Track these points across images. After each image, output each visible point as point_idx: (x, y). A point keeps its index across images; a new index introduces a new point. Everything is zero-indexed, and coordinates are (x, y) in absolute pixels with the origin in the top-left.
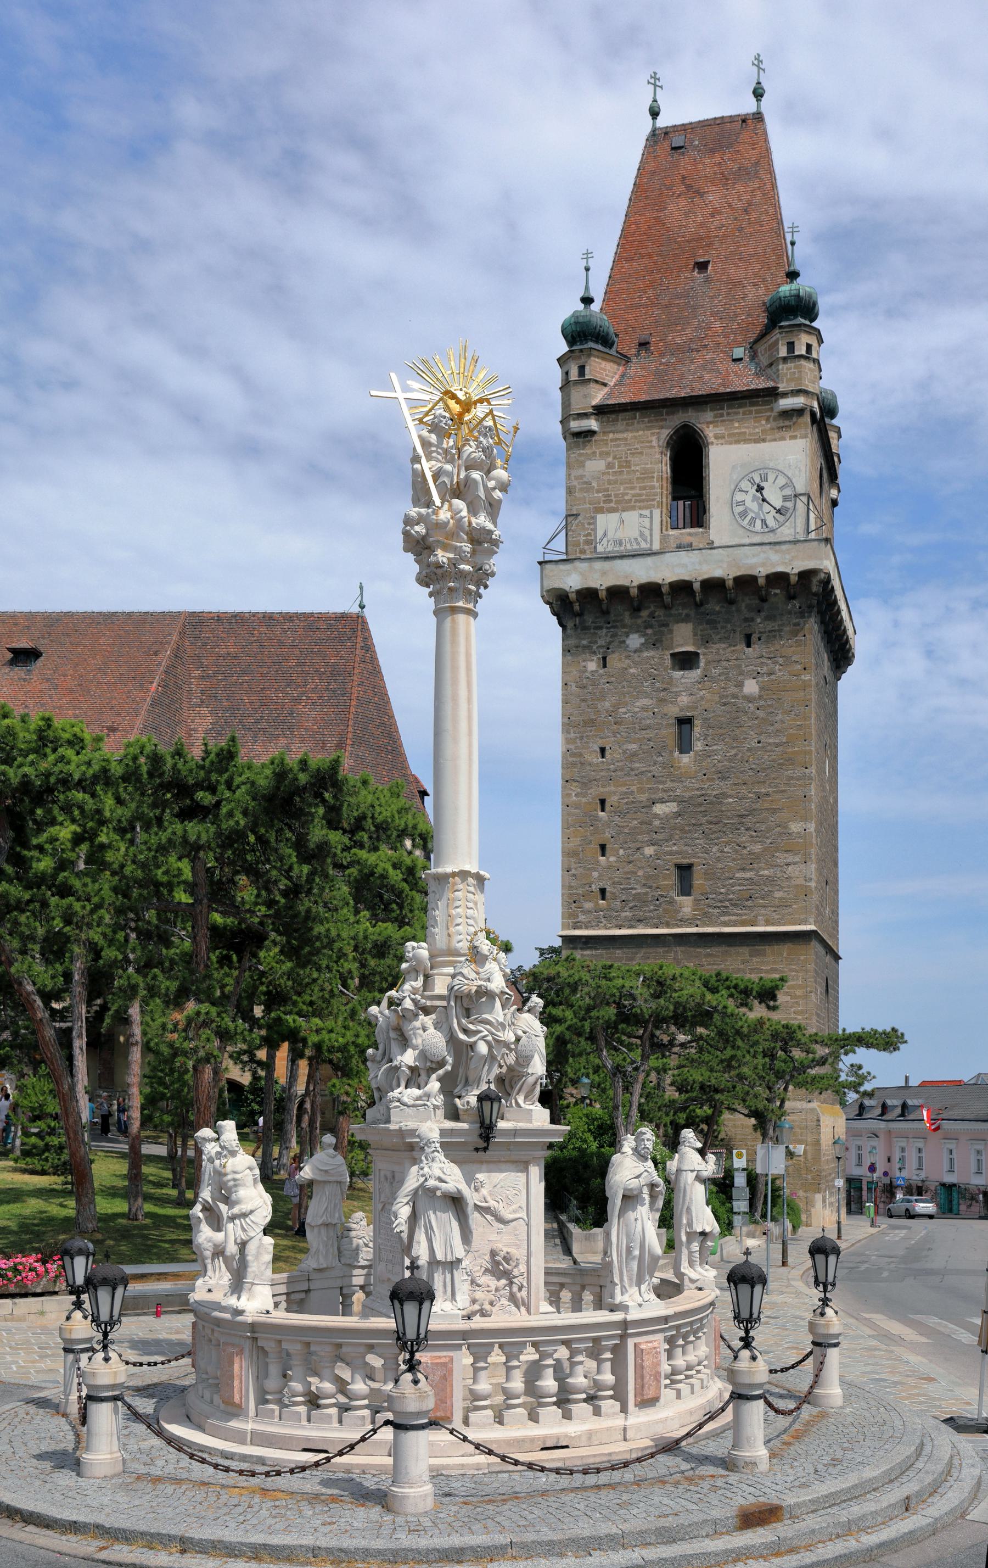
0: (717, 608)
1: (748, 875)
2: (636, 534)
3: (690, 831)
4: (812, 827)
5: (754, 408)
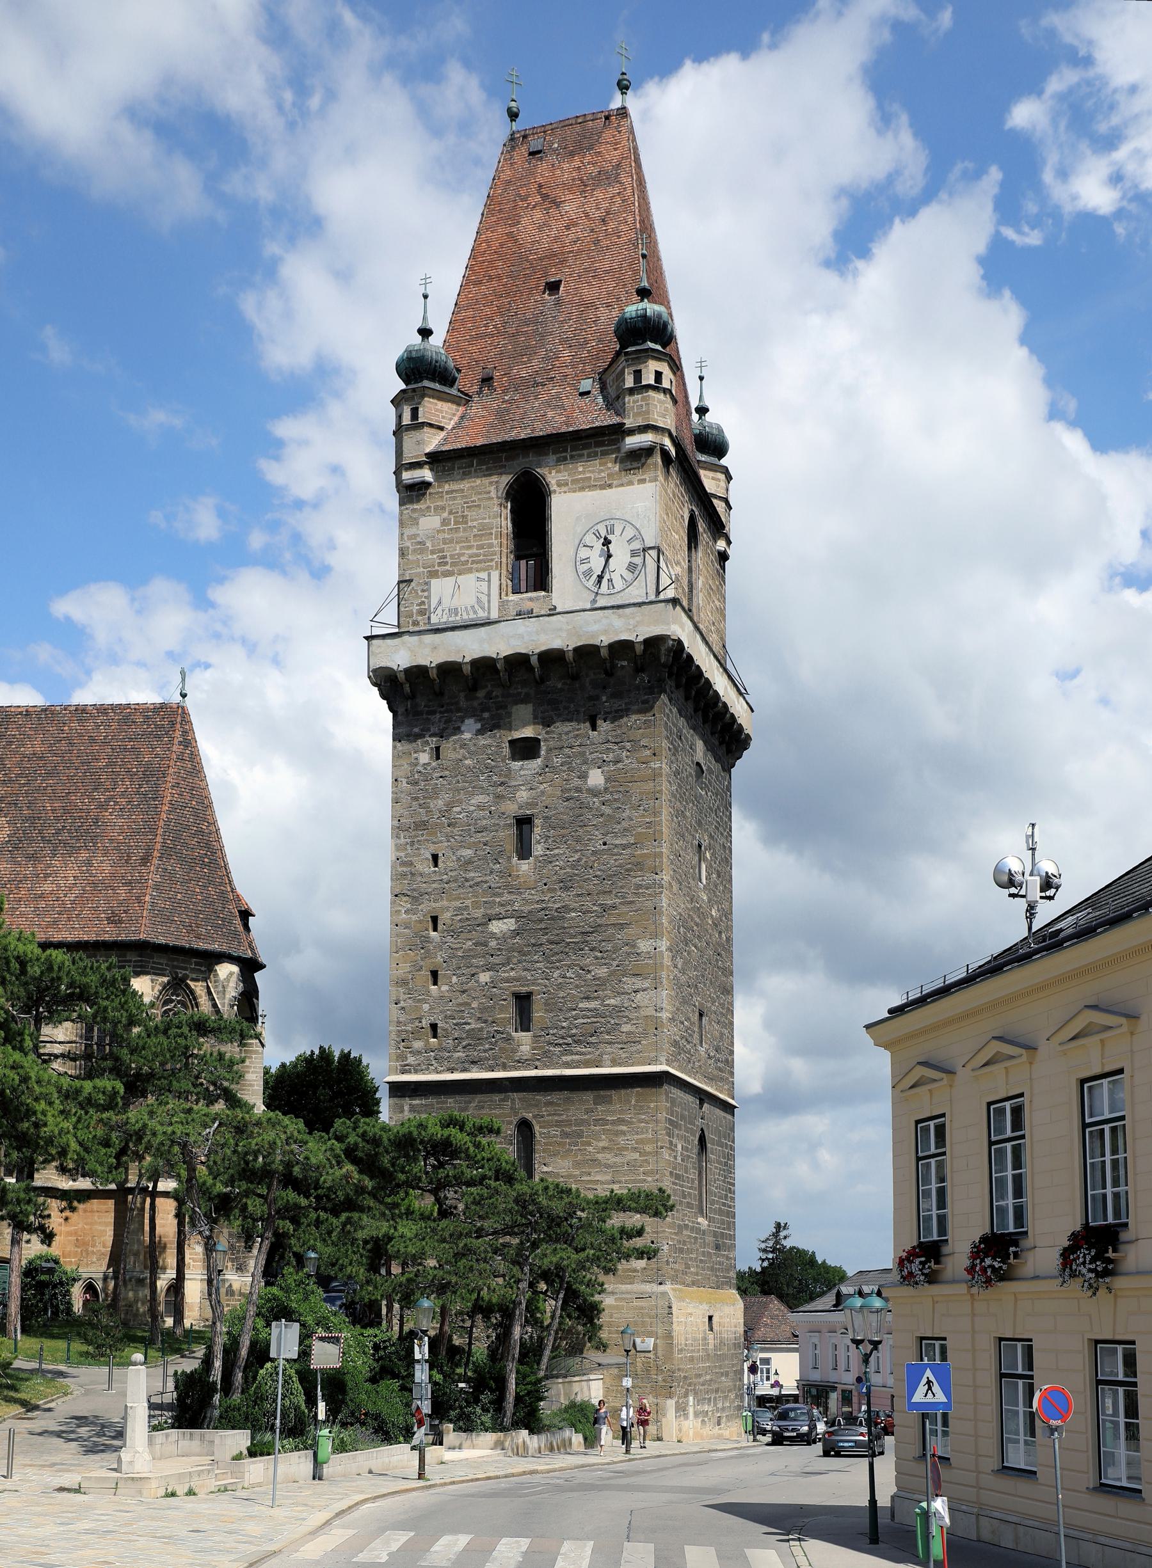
0: (559, 686)
1: (593, 1005)
2: (473, 601)
3: (529, 953)
4: (664, 944)
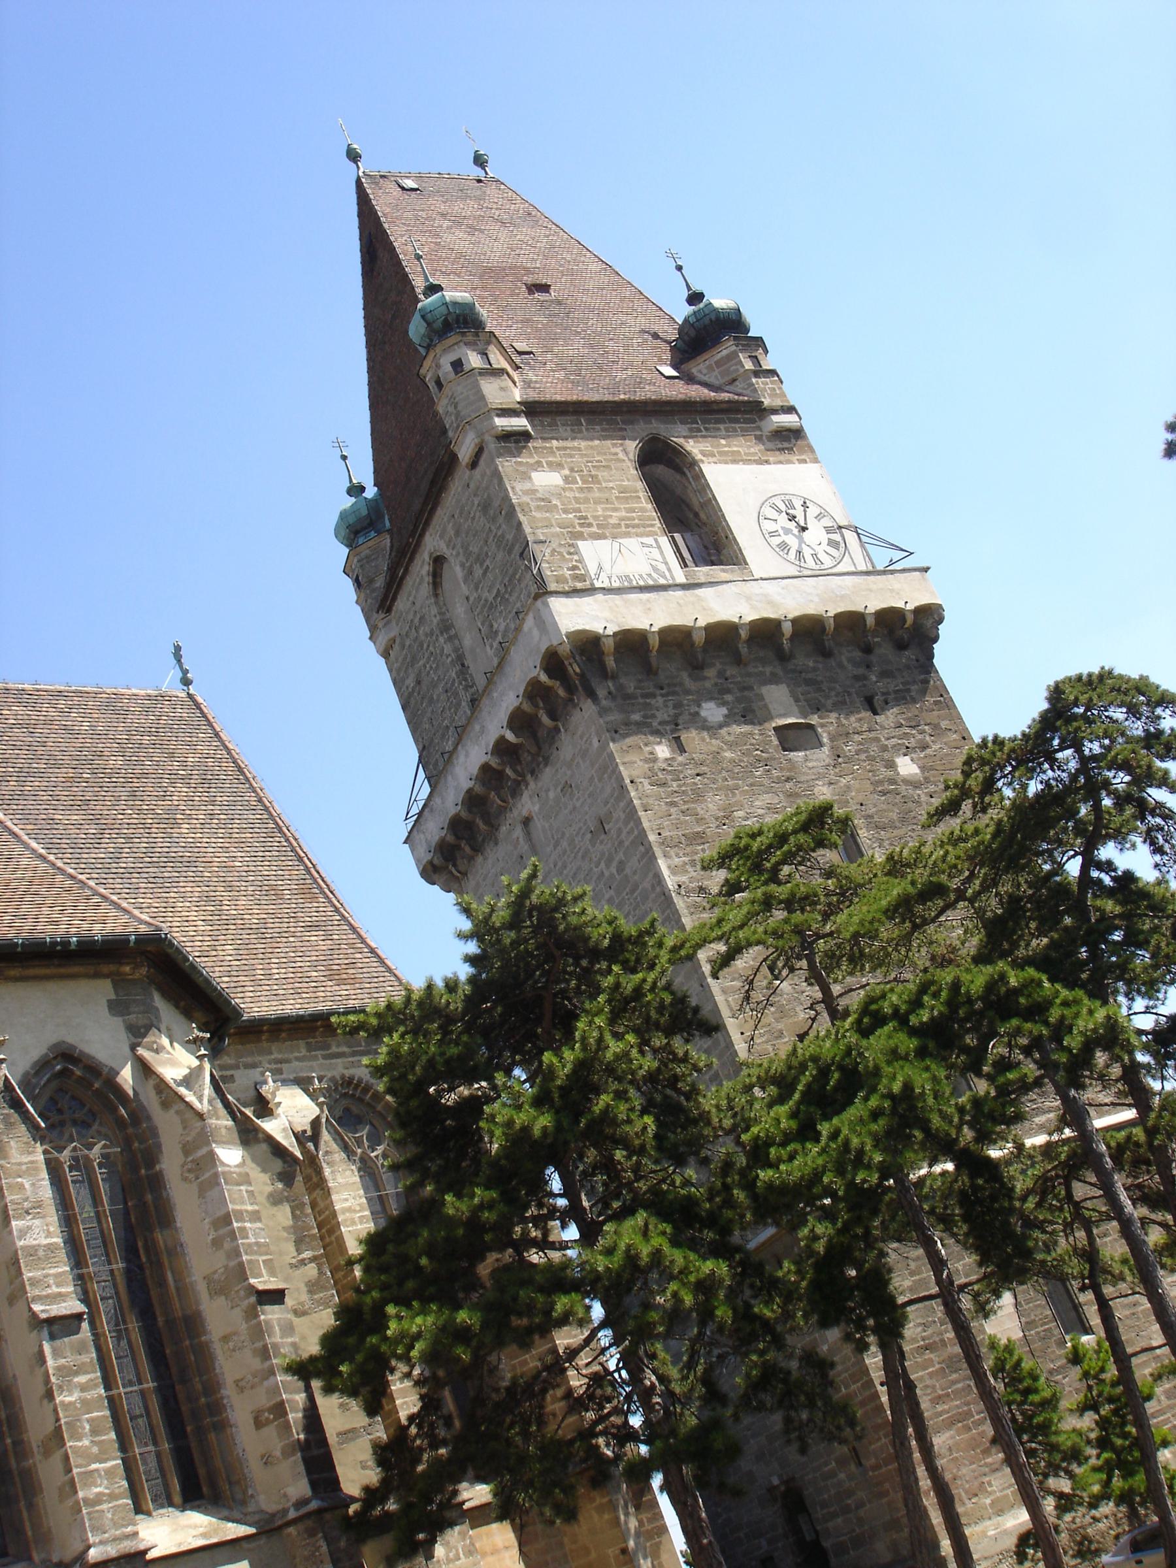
5: (737, 426)
